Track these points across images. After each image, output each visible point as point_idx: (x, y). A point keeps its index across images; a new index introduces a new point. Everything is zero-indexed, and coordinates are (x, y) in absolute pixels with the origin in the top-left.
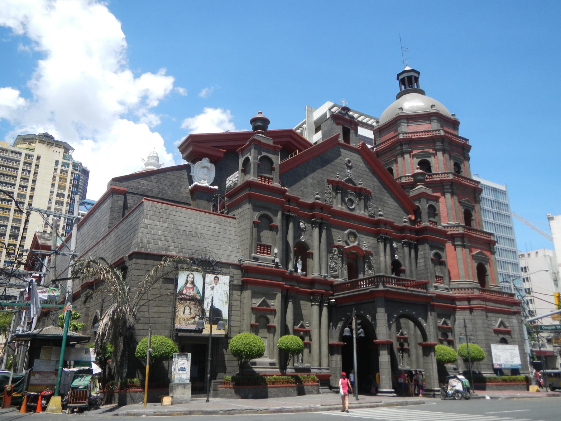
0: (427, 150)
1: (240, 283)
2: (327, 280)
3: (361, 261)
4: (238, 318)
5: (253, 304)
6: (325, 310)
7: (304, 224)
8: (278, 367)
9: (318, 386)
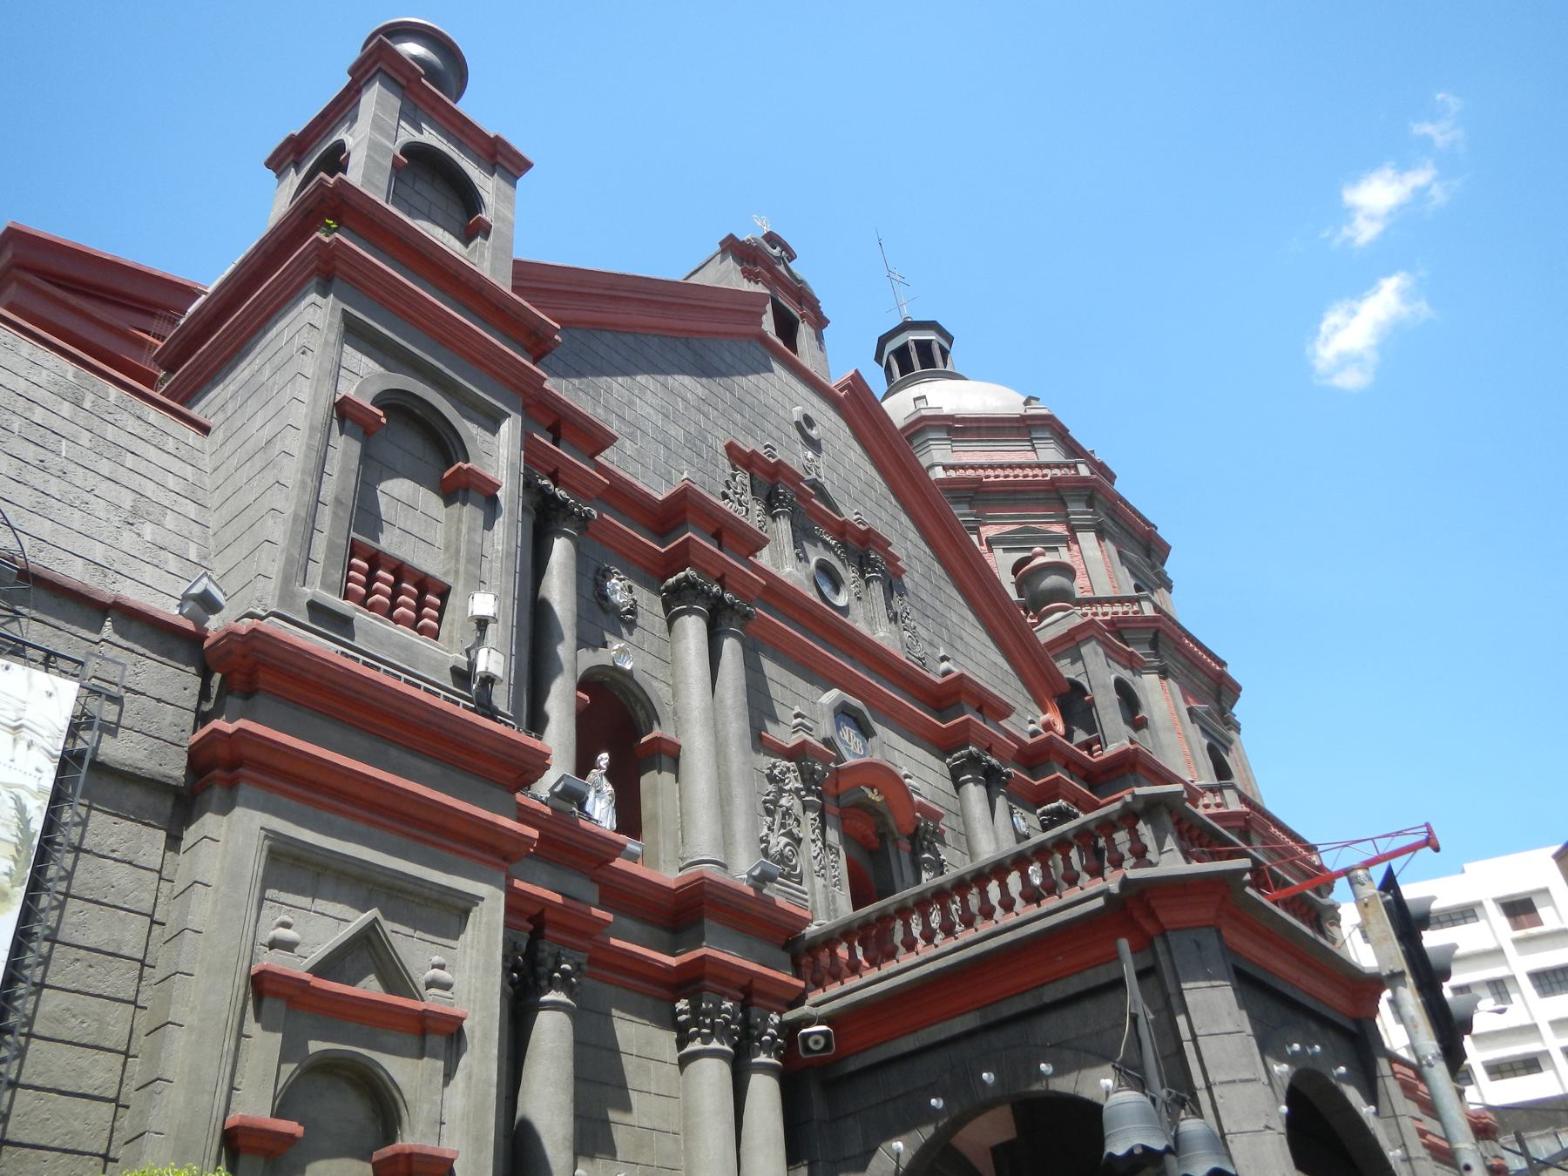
0: (1037, 526)
1: (174, 768)
2: (770, 902)
3: (905, 858)
4: (100, 1073)
5: (274, 944)
6: (764, 1092)
7: (630, 590)
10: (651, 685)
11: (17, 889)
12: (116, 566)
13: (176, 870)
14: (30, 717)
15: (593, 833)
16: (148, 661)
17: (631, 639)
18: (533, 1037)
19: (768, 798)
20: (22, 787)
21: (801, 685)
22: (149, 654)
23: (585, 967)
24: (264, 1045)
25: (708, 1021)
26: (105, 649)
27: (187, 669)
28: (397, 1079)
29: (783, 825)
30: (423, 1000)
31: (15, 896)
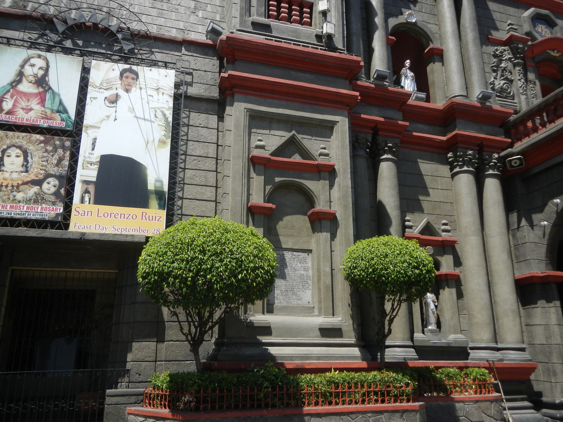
1: (215, 93)
5: (257, 147)
8: (353, 341)
9: (498, 400)
10: (427, 27)
11: (168, 140)
12: (188, 29)
13: (224, 128)
14: (161, 84)
15: (395, 92)
16: (199, 58)
17: (415, 9)
18: (379, 172)
19: (493, 65)
20: (163, 108)
21: (511, 10)
22: (198, 55)
23: (399, 144)
24: (258, 181)
25: (461, 159)
26: (183, 57)
27: (214, 58)
28: (311, 188)
29: (502, 76)
30: (317, 161)
31: (168, 142)
